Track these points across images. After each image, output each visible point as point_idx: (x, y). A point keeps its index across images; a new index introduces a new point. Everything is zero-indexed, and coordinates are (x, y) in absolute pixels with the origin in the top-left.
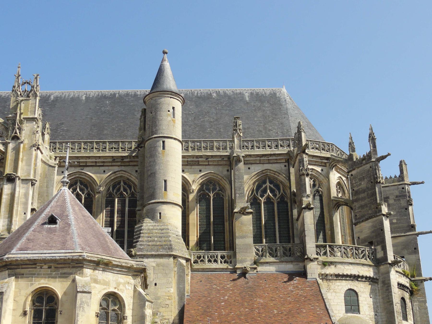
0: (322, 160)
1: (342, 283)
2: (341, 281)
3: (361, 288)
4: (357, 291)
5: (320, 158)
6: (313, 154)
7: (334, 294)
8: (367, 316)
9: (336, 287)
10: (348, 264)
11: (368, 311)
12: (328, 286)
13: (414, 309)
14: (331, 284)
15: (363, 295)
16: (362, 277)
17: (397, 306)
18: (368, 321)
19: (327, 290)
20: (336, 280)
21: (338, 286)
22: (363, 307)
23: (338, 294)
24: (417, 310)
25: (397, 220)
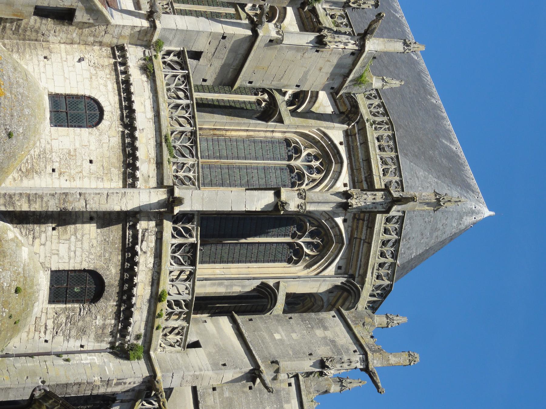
0: (366, 181)
1: (112, 94)
2: (116, 92)
3: (109, 137)
4: (100, 125)
5: (369, 175)
6: (372, 157)
7: (87, 75)
8: (48, 143)
9: (102, 82)
10: (155, 108)
11: (61, 147)
12: (102, 66)
13: (83, 356)
14: (107, 71)
15: (93, 139)
16: (134, 139)
17: (79, 200)
18: (38, 144)
19: (93, 62)
20: (118, 83)
21: (106, 86)
22: (68, 135)
23: (87, 82)
24: (82, 360)
25: (281, 340)
